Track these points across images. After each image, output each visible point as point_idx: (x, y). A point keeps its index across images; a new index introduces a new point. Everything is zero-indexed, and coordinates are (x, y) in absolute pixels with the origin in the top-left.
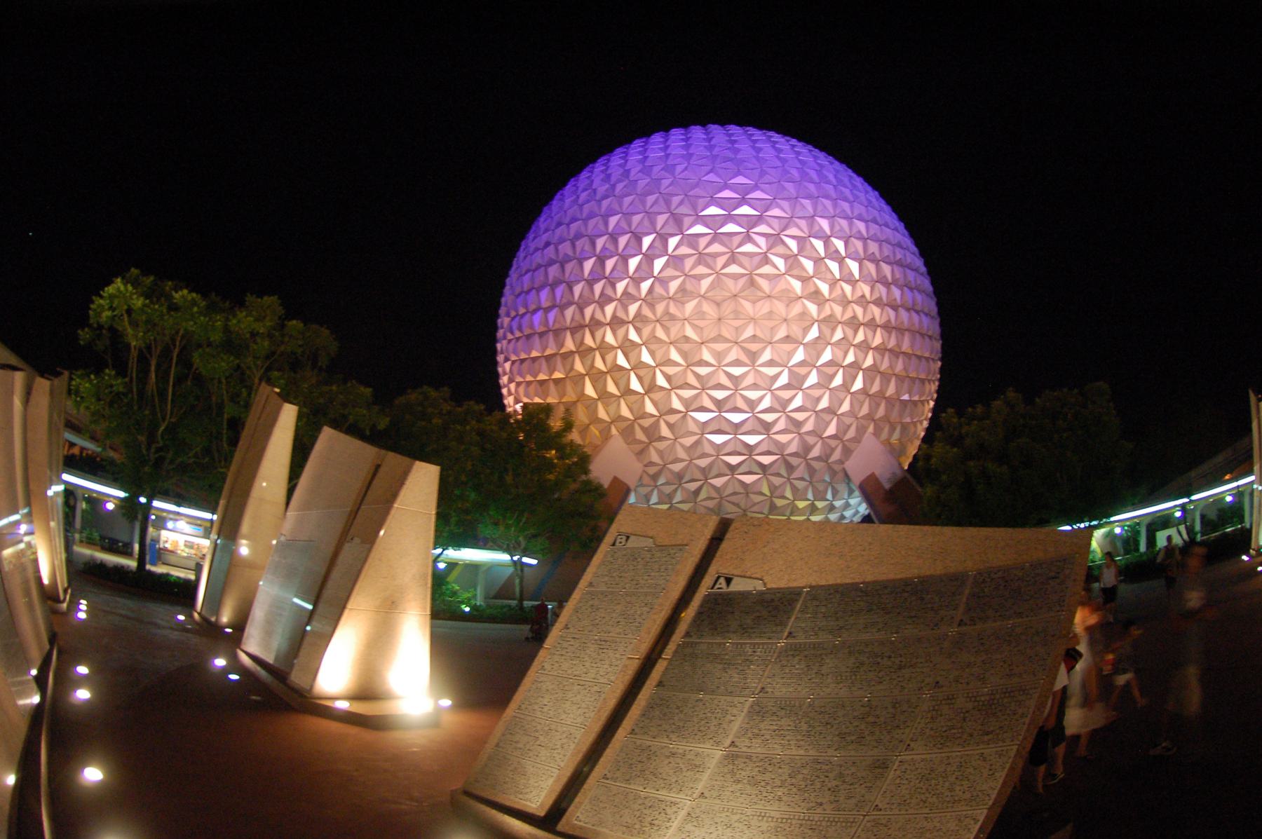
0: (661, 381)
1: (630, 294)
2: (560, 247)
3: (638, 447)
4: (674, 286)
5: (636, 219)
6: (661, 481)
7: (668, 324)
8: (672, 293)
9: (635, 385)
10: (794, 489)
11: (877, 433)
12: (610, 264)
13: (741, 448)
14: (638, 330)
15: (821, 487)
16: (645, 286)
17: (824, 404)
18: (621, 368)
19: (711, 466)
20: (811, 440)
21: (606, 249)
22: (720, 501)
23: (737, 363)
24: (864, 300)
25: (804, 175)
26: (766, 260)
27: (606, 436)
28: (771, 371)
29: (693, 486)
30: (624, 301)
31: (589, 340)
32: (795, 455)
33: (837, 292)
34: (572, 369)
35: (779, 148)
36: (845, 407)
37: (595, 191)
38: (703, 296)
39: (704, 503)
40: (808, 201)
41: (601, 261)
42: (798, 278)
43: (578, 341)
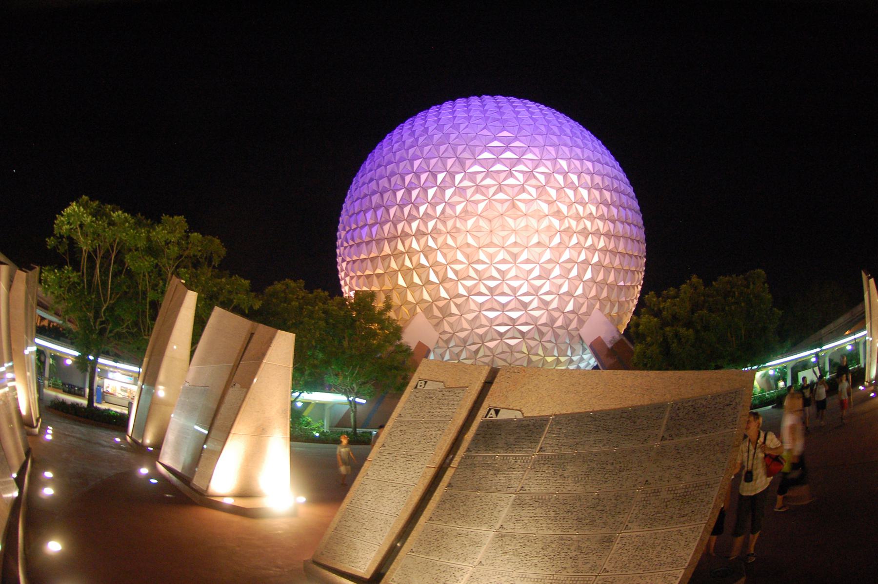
0: (451, 275)
1: (428, 214)
2: (380, 182)
3: (435, 321)
4: (459, 208)
5: (433, 162)
6: (452, 344)
7: (455, 235)
8: (458, 213)
10: (544, 348)
11: (601, 309)
12: (415, 193)
13: (507, 321)
14: (434, 239)
15: (563, 347)
16: (439, 209)
17: (565, 289)
18: (423, 266)
19: (486, 333)
20: (556, 314)
21: (412, 183)
22: (493, 359)
23: (504, 261)
24: (591, 216)
25: (549, 129)
26: (523, 190)
27: (413, 314)
29: (474, 348)
30: (425, 220)
31: (400, 247)
32: (545, 325)
33: (573, 211)
34: (389, 266)
35: (532, 112)
37: (404, 142)
38: (479, 215)
39: (482, 359)
40: (552, 148)
41: (409, 191)
42: (546, 201)
43: (393, 248)
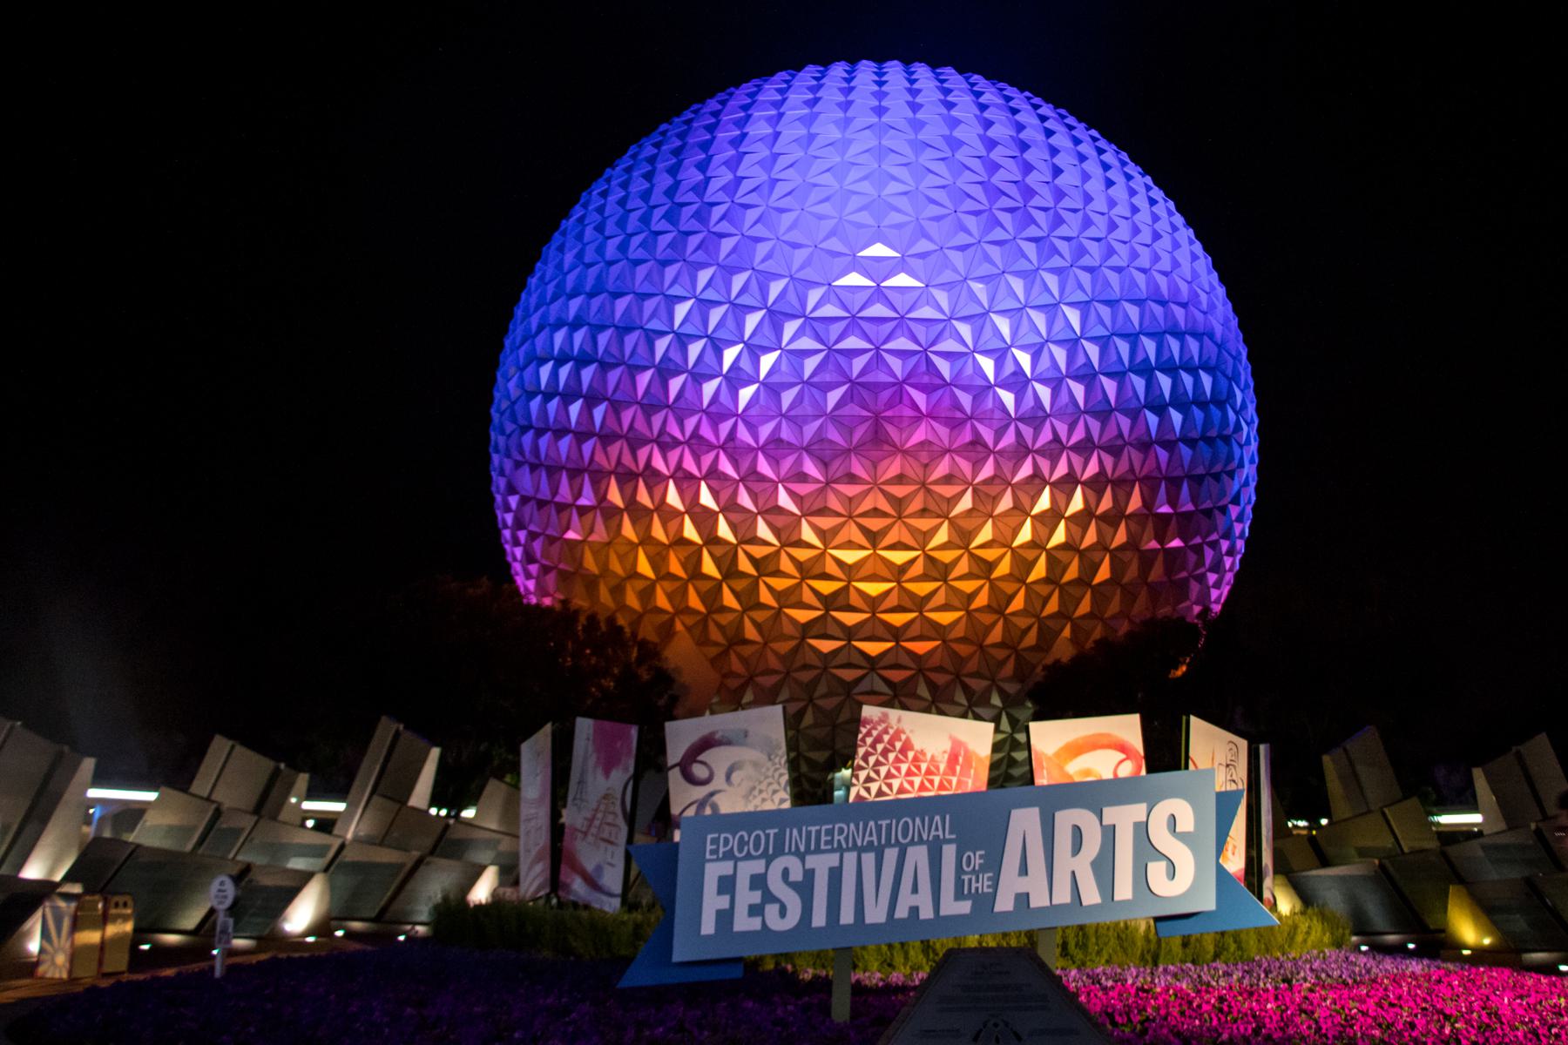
0: (745, 565)
1: (701, 438)
3: (713, 651)
9: (709, 567)
17: (982, 600)
20: (963, 650)
21: (670, 360)
23: (850, 545)
27: (667, 631)
28: (899, 557)
36: (1018, 603)
40: (981, 286)
